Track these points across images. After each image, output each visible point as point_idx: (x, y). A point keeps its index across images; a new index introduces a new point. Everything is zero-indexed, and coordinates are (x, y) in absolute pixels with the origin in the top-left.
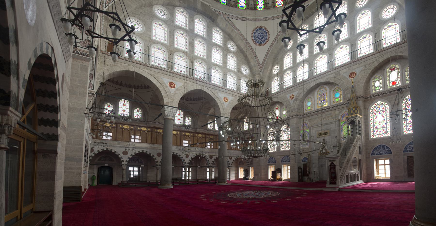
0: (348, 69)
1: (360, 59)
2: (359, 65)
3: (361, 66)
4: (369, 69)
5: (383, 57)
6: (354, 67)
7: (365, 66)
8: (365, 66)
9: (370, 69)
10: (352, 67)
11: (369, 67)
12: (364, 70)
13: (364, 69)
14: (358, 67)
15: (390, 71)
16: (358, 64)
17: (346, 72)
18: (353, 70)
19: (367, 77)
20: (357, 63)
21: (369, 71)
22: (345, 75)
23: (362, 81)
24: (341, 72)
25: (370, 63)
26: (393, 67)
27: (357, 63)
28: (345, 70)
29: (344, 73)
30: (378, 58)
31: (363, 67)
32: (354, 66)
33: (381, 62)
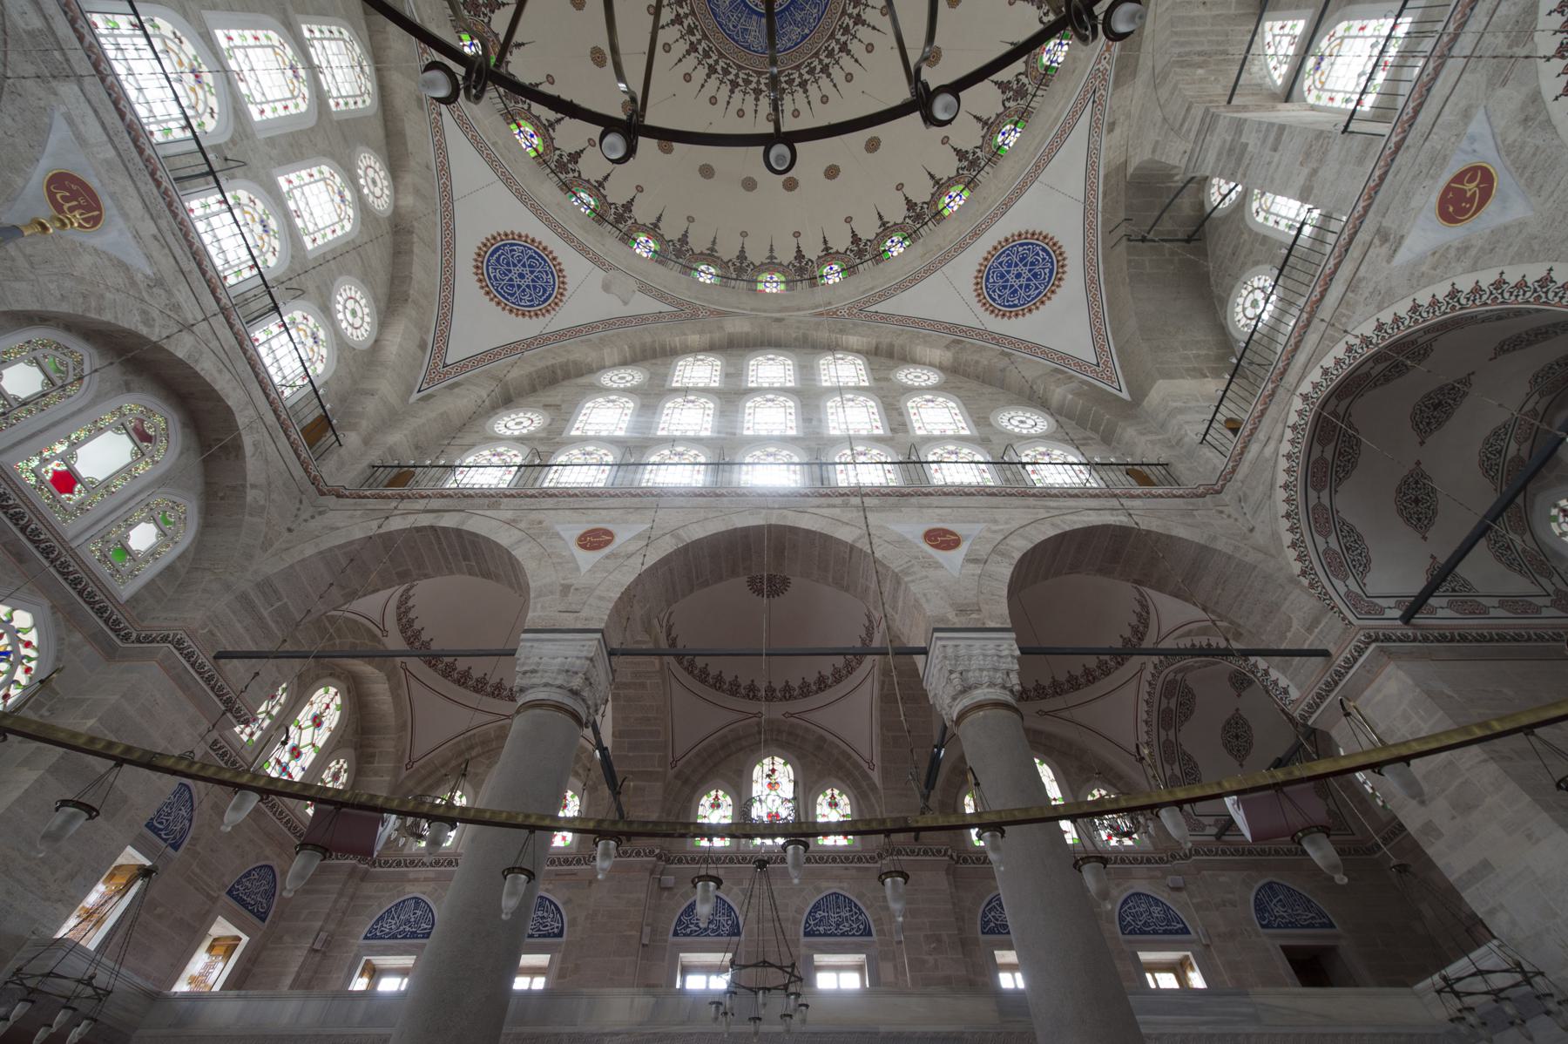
0: (111, 153)
1: (191, 245)
2: (155, 237)
3: (149, 257)
4: (144, 312)
5: (220, 371)
6: (134, 205)
7: (159, 282)
8: (159, 282)
9: (148, 322)
10: (131, 190)
11: (155, 314)
12: (133, 283)
13: (139, 277)
14: (137, 236)
15: (126, 421)
16: (155, 231)
17: (81, 140)
18: (112, 196)
19: (93, 315)
20: (163, 223)
21: (131, 321)
22: (59, 133)
23: (52, 286)
24: (68, 90)
25: (177, 307)
26: (151, 432)
27: (163, 223)
28: (93, 131)
29: (70, 121)
30: (214, 344)
31: (149, 272)
32: (140, 205)
33: (198, 369)
